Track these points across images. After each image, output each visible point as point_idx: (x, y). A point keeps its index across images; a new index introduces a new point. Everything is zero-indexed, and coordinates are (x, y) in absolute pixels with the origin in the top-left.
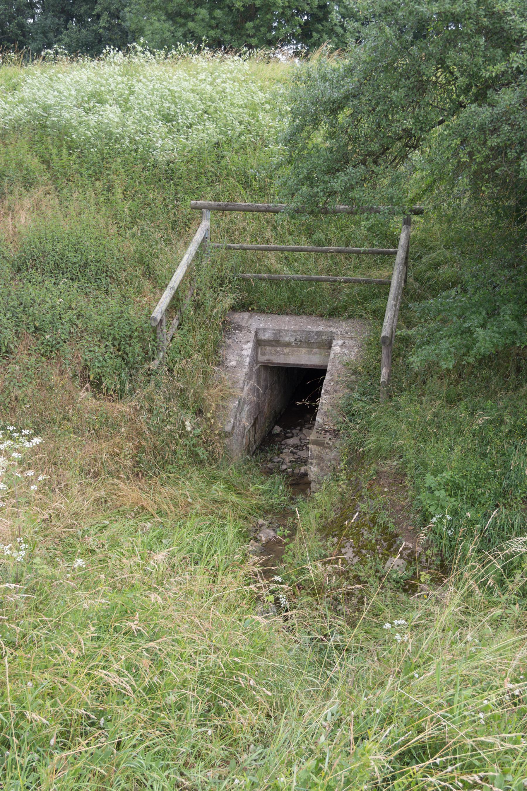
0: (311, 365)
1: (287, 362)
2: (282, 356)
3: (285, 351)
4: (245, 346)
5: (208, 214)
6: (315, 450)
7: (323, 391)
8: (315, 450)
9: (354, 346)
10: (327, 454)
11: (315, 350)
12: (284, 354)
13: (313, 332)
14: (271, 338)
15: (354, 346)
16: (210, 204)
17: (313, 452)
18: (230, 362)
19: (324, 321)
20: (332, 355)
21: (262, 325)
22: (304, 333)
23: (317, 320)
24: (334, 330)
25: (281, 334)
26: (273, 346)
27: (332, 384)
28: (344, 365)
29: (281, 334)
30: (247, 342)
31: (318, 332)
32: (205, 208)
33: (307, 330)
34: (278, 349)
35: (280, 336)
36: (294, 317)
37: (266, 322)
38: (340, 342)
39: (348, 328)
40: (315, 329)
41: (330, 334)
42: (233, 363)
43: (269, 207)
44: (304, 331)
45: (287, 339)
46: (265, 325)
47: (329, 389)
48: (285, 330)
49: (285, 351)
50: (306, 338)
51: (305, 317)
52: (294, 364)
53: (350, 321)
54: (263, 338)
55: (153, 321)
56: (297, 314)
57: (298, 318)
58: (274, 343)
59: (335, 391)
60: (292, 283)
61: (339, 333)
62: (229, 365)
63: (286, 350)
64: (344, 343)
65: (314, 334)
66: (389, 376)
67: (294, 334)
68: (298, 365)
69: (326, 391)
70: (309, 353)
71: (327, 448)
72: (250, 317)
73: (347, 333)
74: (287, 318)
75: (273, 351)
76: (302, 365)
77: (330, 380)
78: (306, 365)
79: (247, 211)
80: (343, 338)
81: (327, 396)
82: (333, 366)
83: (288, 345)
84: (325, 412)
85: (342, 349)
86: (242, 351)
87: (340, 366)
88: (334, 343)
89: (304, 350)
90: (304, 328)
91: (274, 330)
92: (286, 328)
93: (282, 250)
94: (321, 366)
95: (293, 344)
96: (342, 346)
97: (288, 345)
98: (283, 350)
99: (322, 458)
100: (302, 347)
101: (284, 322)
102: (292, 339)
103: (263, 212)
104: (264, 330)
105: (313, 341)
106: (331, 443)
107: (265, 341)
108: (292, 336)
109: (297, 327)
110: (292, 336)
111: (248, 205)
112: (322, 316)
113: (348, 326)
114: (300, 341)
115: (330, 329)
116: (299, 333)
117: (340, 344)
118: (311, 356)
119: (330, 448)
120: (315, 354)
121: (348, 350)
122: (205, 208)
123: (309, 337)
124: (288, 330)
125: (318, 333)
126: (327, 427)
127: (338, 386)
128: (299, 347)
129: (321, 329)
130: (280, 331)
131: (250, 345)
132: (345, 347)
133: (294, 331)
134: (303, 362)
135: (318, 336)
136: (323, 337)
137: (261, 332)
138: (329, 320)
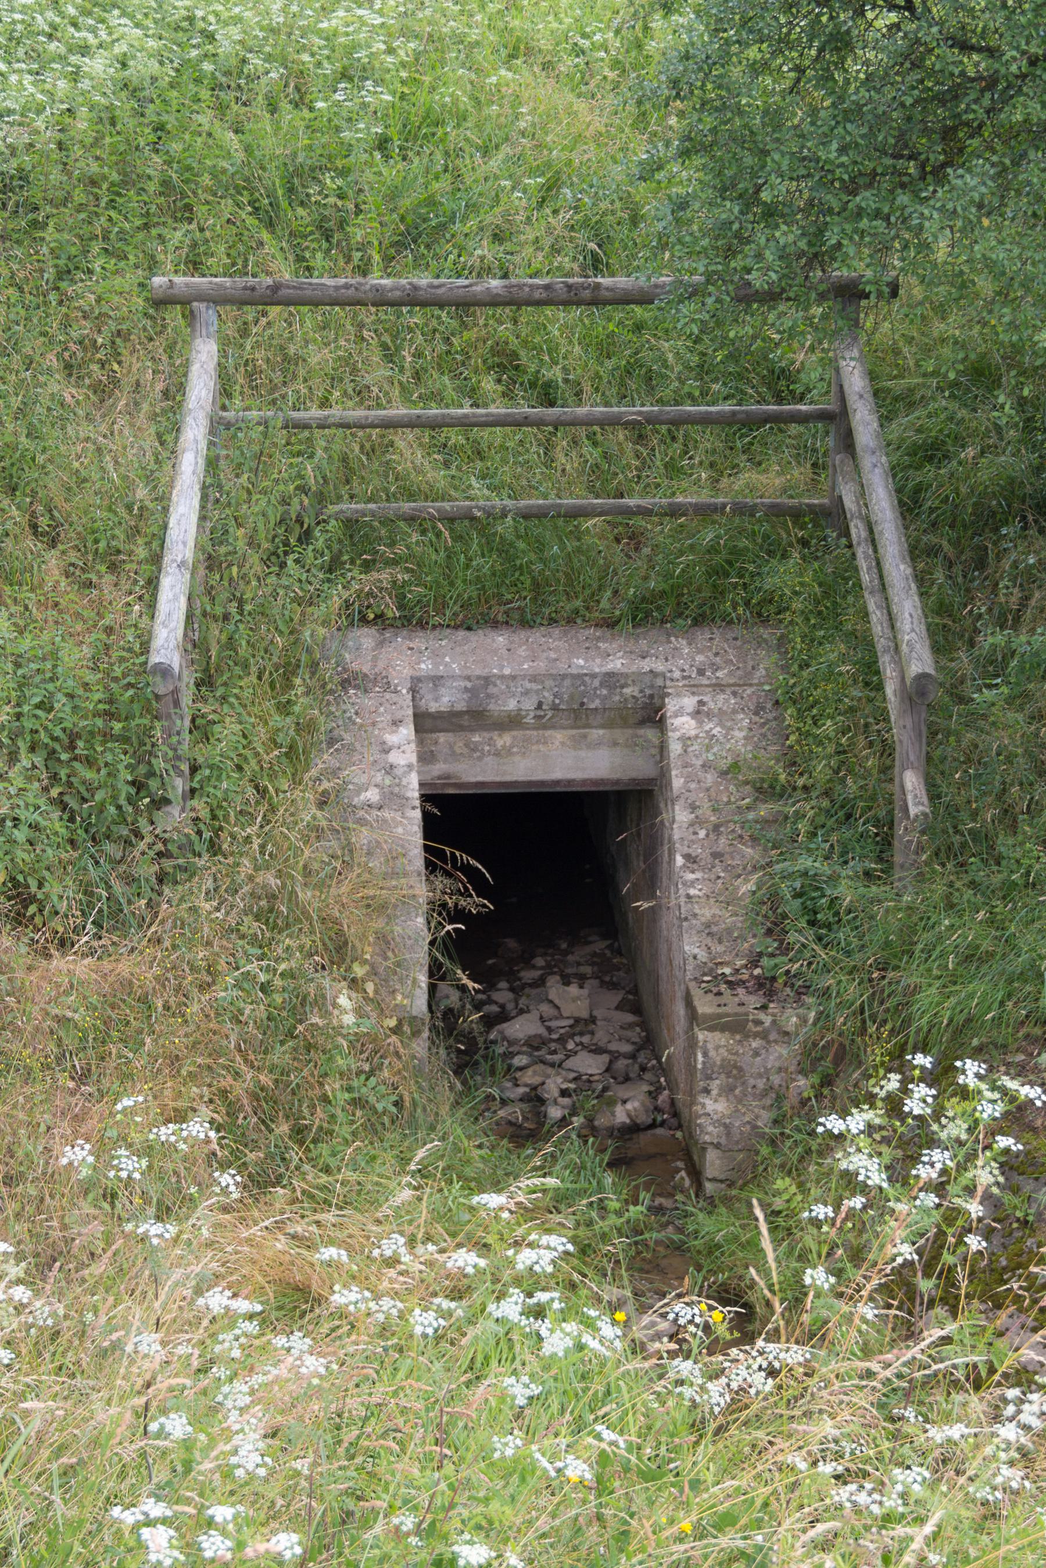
0: (584, 782)
1: (508, 778)
2: (489, 760)
3: (500, 743)
4: (392, 739)
5: (207, 313)
6: (717, 1048)
7: (679, 860)
8: (717, 1048)
9: (734, 712)
10: (756, 1054)
11: (597, 733)
12: (497, 754)
13: (593, 676)
14: (461, 706)
15: (734, 712)
16: (220, 286)
17: (712, 1053)
18: (358, 793)
19: (621, 641)
20: (675, 748)
21: (425, 667)
22: (567, 682)
23: (598, 639)
24: (660, 667)
25: (492, 690)
26: (462, 728)
27: (702, 834)
28: (724, 774)
29: (492, 690)
30: (396, 723)
31: (610, 675)
32: (201, 298)
33: (574, 671)
34: (476, 738)
35: (489, 696)
36: (523, 634)
37: (436, 655)
38: (689, 702)
39: (700, 658)
40: (598, 666)
41: (647, 679)
42: (372, 795)
43: (415, 288)
44: (564, 677)
45: (512, 705)
46: (436, 665)
47: (697, 850)
48: (502, 677)
49: (500, 743)
50: (572, 697)
51: (556, 632)
52: (530, 783)
53: (702, 636)
54: (433, 707)
55: (158, 679)
56: (526, 624)
57: (535, 636)
58: (465, 721)
59: (716, 855)
60: (505, 528)
61: (677, 674)
62: (356, 801)
63: (502, 740)
64: (701, 703)
65: (596, 683)
66: (934, 795)
67: (535, 686)
68: (542, 783)
69: (687, 857)
70: (577, 743)
71: (756, 1035)
72: (381, 644)
73: (701, 672)
74: (500, 639)
75: (459, 747)
76: (558, 782)
77: (692, 824)
78: (570, 782)
79: (304, 304)
80: (694, 689)
81: (698, 875)
82: (689, 779)
83: (512, 722)
84: (708, 925)
85: (700, 723)
86: (387, 751)
87: (710, 778)
88: (671, 705)
89: (558, 736)
90: (562, 667)
91: (468, 678)
92: (507, 671)
93: (435, 425)
94: (617, 782)
95: (529, 720)
96: (697, 714)
97: (512, 722)
98: (491, 742)
99: (740, 1069)
100: (553, 727)
101: (495, 651)
102: (529, 704)
103: (392, 304)
104: (437, 680)
105: (596, 704)
106: (767, 1020)
107: (439, 716)
108: (526, 693)
109: (541, 665)
110: (526, 693)
111: (347, 286)
112: (610, 624)
113: (700, 652)
114: (555, 708)
115: (646, 665)
116: (549, 683)
117: (690, 710)
118: (583, 753)
119: (764, 1035)
120: (598, 744)
121: (721, 724)
122: (201, 298)
123: (584, 694)
124: (513, 678)
125: (611, 680)
126: (727, 971)
127: (723, 840)
128: (545, 727)
129: (616, 664)
130: (487, 680)
131: (407, 731)
132: (709, 715)
133: (534, 679)
134: (557, 774)
135: (611, 688)
136: (627, 691)
137: (425, 688)
138: (637, 638)
